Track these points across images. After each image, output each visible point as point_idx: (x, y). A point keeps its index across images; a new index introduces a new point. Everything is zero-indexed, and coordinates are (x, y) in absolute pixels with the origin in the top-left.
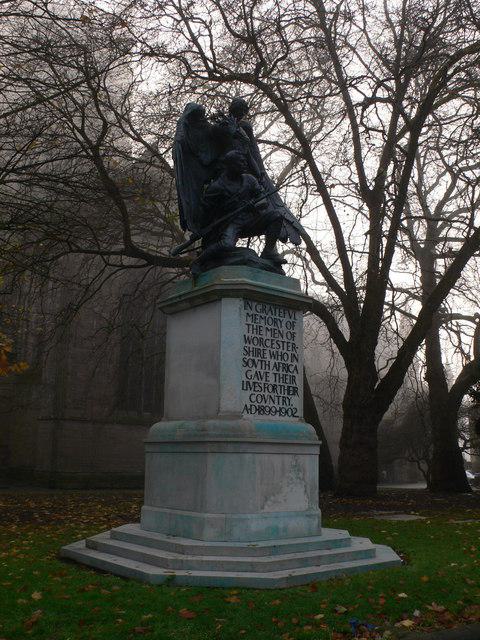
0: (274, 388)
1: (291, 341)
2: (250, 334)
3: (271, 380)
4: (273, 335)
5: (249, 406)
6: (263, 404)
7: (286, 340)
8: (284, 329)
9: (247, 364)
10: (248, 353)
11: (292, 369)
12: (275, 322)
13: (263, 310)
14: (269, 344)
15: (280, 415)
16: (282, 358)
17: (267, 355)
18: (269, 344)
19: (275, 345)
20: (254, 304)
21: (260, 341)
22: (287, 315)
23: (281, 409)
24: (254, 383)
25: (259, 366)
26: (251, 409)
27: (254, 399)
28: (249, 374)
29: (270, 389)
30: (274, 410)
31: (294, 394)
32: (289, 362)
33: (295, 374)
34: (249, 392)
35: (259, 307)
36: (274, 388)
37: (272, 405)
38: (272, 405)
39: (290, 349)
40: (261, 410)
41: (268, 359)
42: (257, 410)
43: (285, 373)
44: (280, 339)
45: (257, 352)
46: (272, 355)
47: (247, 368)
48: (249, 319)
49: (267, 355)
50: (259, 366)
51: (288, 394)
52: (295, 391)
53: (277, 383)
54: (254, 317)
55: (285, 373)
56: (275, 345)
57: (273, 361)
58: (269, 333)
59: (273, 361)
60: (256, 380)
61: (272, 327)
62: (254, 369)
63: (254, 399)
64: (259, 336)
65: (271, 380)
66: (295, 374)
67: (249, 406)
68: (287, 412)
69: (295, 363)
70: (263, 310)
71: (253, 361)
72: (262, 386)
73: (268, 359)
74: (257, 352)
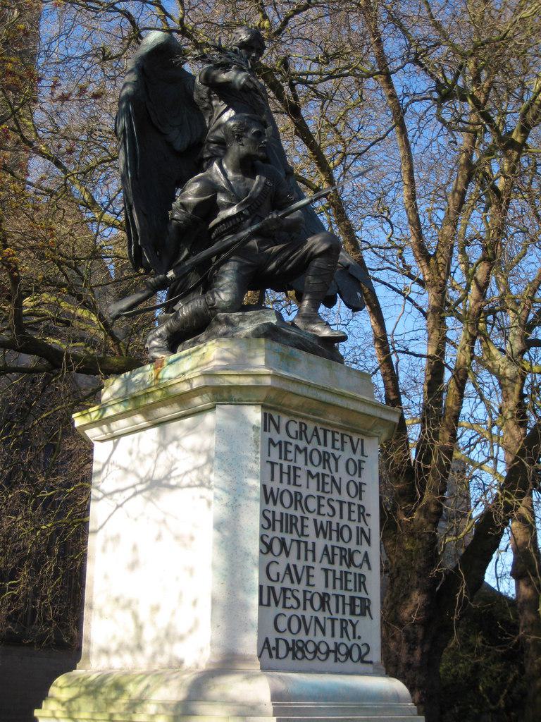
0: (324, 599)
1: (356, 501)
4: (321, 487)
5: (273, 644)
6: (302, 636)
8: (342, 476)
11: (358, 559)
12: (324, 459)
13: (302, 433)
14: (312, 504)
15: (336, 660)
17: (310, 530)
18: (312, 504)
19: (326, 510)
20: (284, 420)
21: (297, 500)
22: (348, 446)
23: (337, 646)
24: (284, 590)
25: (294, 552)
26: (277, 649)
27: (283, 624)
28: (274, 570)
29: (317, 603)
31: (363, 614)
32: (352, 545)
36: (324, 599)
37: (319, 637)
38: (319, 637)
39: (355, 516)
41: (312, 538)
42: (288, 649)
43: (344, 568)
44: (335, 496)
45: (290, 523)
46: (321, 530)
47: (270, 557)
48: (275, 451)
49: (310, 530)
50: (294, 552)
51: (353, 613)
52: (366, 608)
53: (330, 591)
54: (283, 447)
55: (344, 568)
56: (326, 510)
57: (321, 543)
58: (313, 483)
60: (287, 584)
61: (320, 470)
62: (283, 560)
63: (283, 624)
64: (293, 489)
66: (364, 570)
68: (349, 653)
71: (283, 542)
73: (312, 538)
74: (290, 523)
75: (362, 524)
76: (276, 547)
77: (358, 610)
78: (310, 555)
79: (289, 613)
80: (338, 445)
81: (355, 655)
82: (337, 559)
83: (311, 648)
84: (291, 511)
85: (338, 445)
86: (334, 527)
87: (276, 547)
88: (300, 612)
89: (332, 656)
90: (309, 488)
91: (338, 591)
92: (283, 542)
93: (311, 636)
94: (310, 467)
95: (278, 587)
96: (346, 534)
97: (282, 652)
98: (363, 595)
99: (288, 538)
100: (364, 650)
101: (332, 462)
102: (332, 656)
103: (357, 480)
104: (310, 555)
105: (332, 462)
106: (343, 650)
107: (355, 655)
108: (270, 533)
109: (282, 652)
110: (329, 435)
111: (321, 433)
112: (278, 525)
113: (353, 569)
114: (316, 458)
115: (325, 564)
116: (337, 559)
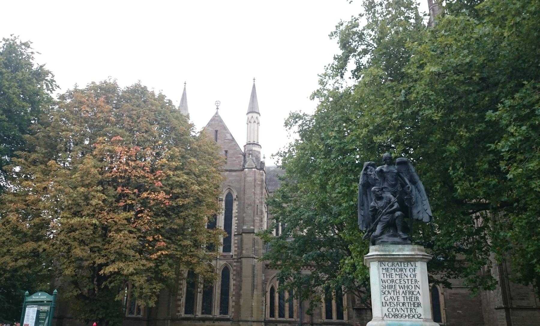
0: (403, 304)
2: (385, 279)
3: (401, 300)
5: (387, 314)
6: (397, 312)
7: (410, 278)
8: (408, 273)
9: (384, 293)
10: (385, 288)
11: (415, 293)
12: (401, 270)
13: (392, 265)
14: (398, 281)
16: (408, 287)
17: (398, 288)
20: (387, 263)
21: (392, 281)
23: (409, 315)
27: (390, 310)
28: (386, 298)
29: (401, 305)
30: (404, 315)
31: (418, 306)
32: (413, 290)
33: (418, 295)
34: (387, 307)
35: (390, 264)
36: (403, 304)
38: (403, 312)
39: (414, 282)
40: (395, 316)
43: (410, 295)
44: (406, 278)
47: (385, 295)
48: (384, 271)
49: (398, 288)
52: (419, 305)
53: (406, 301)
54: (387, 270)
57: (401, 291)
58: (398, 277)
59: (401, 291)
60: (391, 301)
61: (400, 273)
62: (389, 296)
63: (390, 310)
64: (391, 279)
65: (401, 300)
66: (418, 295)
67: (387, 314)
68: (413, 316)
69: (418, 290)
70: (392, 265)
71: (389, 292)
72: (396, 304)
75: (416, 284)
76: (387, 293)
77: (416, 306)
78: (398, 294)
79: (392, 308)
80: (406, 265)
81: (416, 316)
82: (408, 294)
83: (400, 315)
84: (391, 284)
85: (406, 265)
86: (406, 286)
87: (387, 293)
88: (396, 307)
89: (407, 317)
90: (395, 277)
91: (408, 301)
92: (389, 292)
93: (400, 312)
94: (396, 273)
95: (388, 302)
96: (410, 287)
97: (391, 316)
98: (418, 302)
99: (390, 291)
100: (419, 315)
101: (404, 270)
102: (407, 317)
103: (414, 273)
104: (398, 294)
105: (404, 270)
106: (411, 315)
107: (416, 316)
108: (384, 290)
109: (391, 316)
110: (402, 264)
111: (400, 264)
112: (387, 288)
113: (413, 296)
114: (398, 270)
115: (403, 295)
116: (408, 294)
